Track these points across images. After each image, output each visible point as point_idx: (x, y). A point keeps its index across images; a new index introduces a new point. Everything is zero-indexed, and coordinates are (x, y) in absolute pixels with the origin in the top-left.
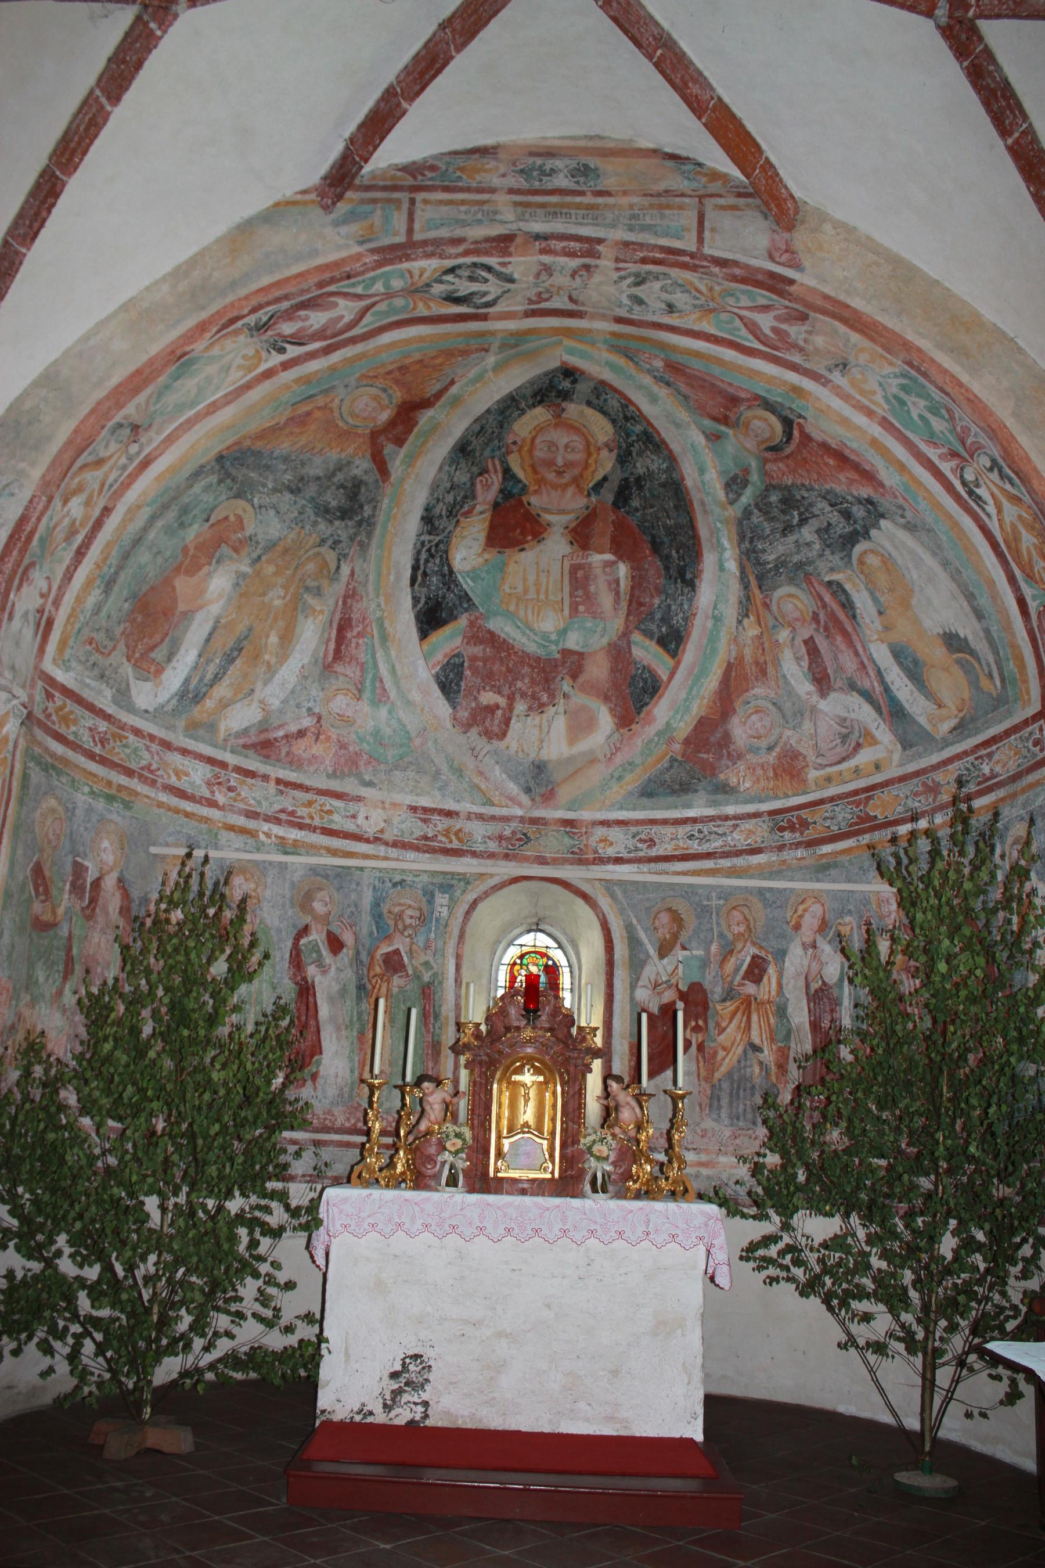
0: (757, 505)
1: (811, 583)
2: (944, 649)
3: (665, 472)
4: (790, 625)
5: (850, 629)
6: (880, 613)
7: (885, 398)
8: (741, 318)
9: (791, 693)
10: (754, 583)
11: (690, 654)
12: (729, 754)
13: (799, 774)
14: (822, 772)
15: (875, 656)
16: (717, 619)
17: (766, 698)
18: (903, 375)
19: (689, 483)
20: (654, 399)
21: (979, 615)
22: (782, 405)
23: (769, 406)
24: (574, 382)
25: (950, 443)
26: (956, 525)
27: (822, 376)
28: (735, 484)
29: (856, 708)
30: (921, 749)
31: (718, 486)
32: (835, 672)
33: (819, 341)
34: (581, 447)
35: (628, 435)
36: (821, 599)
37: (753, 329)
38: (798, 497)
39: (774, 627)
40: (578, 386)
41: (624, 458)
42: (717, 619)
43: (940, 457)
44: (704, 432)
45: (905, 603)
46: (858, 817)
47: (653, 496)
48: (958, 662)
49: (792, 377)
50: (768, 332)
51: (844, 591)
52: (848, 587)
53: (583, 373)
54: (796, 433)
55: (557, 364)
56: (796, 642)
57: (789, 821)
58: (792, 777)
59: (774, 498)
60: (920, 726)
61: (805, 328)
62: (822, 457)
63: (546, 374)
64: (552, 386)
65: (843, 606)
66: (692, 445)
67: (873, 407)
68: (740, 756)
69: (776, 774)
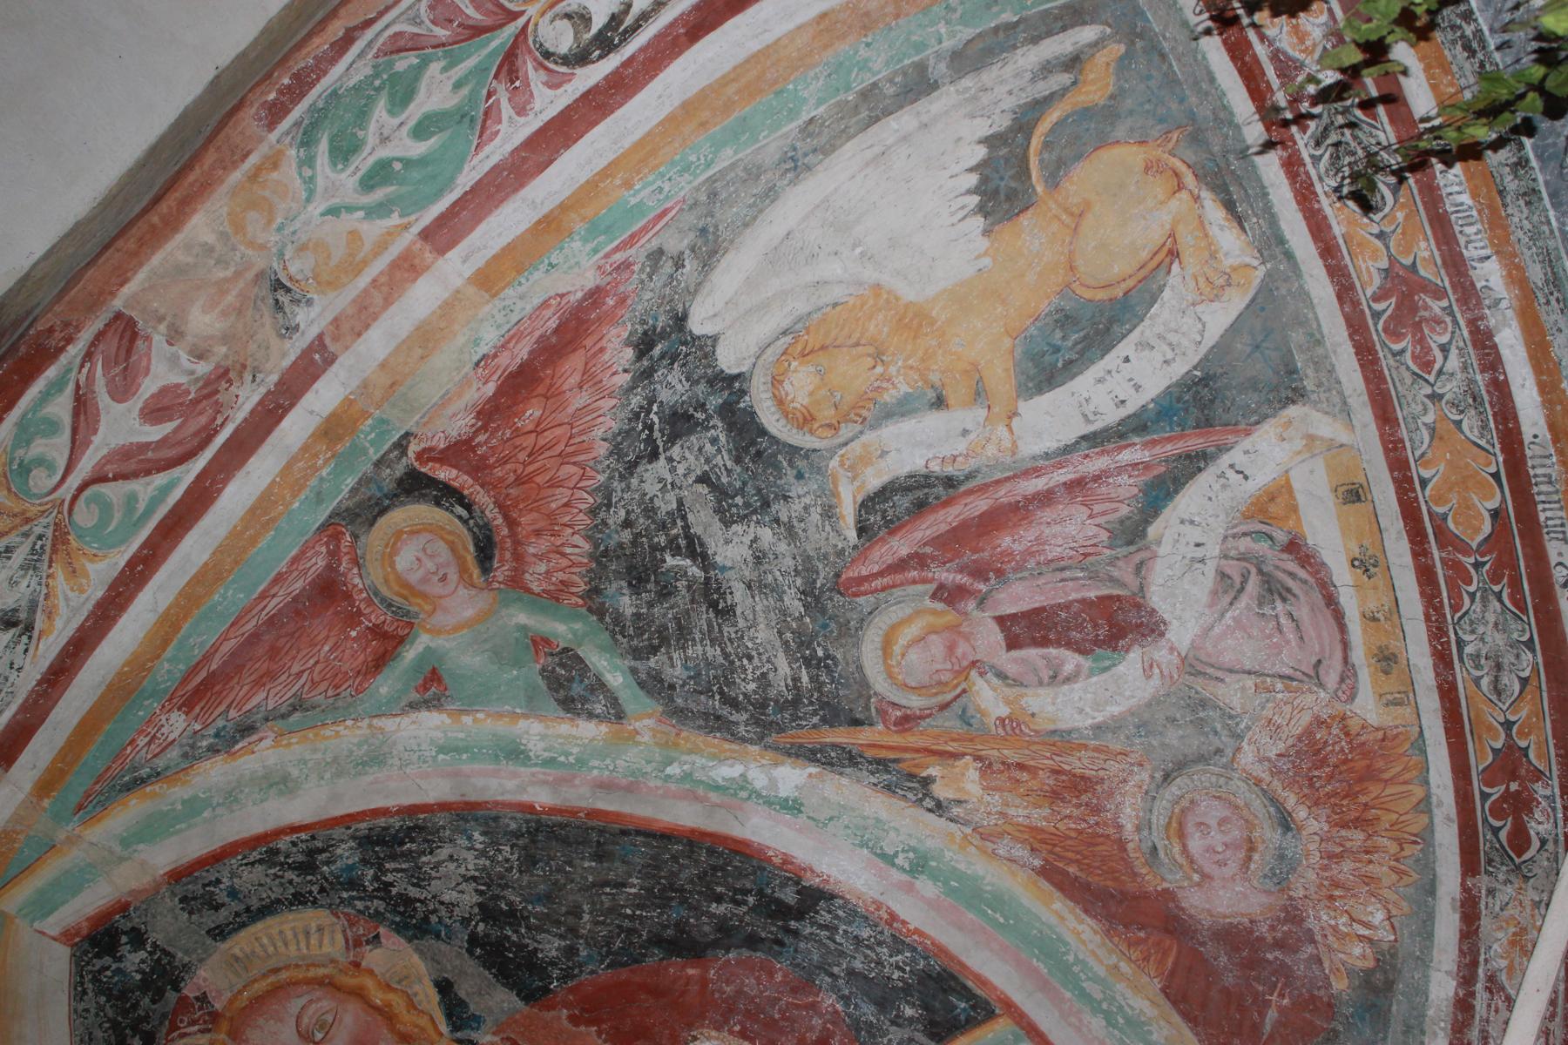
0: (637, 654)
1: (862, 580)
2: (1025, 220)
3: (495, 843)
4: (962, 673)
5: (981, 505)
6: (940, 403)
7: (379, 210)
8: (99, 478)
9: (1142, 722)
10: (840, 736)
11: (990, 966)
12: (1279, 944)
13: (1363, 750)
14: (1365, 676)
15: (1050, 444)
16: (920, 865)
17: (1150, 798)
18: (307, 141)
19: (542, 797)
20: (281, 783)
21: (918, 85)
22: (364, 481)
23: (364, 511)
24: (138, 938)
25: (480, 70)
26: (690, 110)
27: (307, 353)
28: (568, 685)
29: (1195, 535)
30: (1297, 337)
31: (565, 728)
32: (1094, 576)
33: (202, 321)
34: (326, 1004)
35: (353, 884)
36: (900, 566)
37: (133, 463)
38: (626, 536)
39: (964, 718)
40: (155, 936)
41: (415, 922)
42: (920, 865)
43: (521, 111)
44: (413, 706)
45: (913, 320)
46: (1495, 578)
47: (548, 898)
48: (1053, 181)
49: (296, 427)
50: (154, 433)
51: (884, 493)
52: (874, 482)
53: (123, 908)
54: (444, 474)
55: (63, 953)
56: (1012, 669)
57: (1497, 811)
58: (1370, 775)
59: (627, 604)
60: (1234, 329)
61: (158, 340)
62: (518, 433)
63: (79, 993)
64: (120, 996)
65: (921, 507)
66: (442, 749)
67: (395, 251)
68: (1293, 915)
69: (1359, 823)
